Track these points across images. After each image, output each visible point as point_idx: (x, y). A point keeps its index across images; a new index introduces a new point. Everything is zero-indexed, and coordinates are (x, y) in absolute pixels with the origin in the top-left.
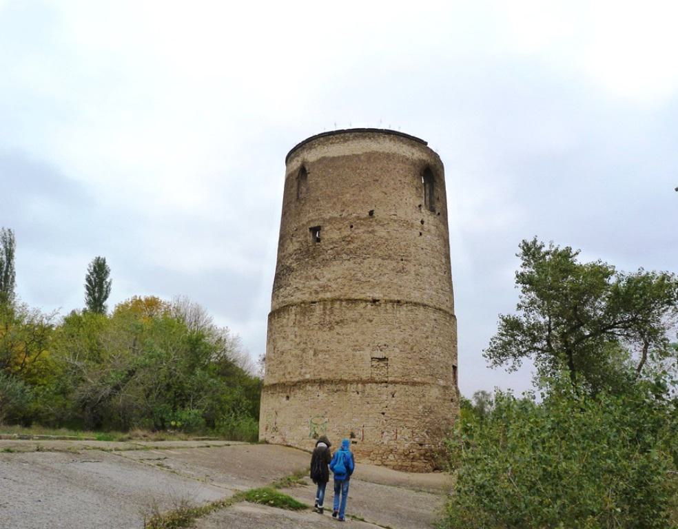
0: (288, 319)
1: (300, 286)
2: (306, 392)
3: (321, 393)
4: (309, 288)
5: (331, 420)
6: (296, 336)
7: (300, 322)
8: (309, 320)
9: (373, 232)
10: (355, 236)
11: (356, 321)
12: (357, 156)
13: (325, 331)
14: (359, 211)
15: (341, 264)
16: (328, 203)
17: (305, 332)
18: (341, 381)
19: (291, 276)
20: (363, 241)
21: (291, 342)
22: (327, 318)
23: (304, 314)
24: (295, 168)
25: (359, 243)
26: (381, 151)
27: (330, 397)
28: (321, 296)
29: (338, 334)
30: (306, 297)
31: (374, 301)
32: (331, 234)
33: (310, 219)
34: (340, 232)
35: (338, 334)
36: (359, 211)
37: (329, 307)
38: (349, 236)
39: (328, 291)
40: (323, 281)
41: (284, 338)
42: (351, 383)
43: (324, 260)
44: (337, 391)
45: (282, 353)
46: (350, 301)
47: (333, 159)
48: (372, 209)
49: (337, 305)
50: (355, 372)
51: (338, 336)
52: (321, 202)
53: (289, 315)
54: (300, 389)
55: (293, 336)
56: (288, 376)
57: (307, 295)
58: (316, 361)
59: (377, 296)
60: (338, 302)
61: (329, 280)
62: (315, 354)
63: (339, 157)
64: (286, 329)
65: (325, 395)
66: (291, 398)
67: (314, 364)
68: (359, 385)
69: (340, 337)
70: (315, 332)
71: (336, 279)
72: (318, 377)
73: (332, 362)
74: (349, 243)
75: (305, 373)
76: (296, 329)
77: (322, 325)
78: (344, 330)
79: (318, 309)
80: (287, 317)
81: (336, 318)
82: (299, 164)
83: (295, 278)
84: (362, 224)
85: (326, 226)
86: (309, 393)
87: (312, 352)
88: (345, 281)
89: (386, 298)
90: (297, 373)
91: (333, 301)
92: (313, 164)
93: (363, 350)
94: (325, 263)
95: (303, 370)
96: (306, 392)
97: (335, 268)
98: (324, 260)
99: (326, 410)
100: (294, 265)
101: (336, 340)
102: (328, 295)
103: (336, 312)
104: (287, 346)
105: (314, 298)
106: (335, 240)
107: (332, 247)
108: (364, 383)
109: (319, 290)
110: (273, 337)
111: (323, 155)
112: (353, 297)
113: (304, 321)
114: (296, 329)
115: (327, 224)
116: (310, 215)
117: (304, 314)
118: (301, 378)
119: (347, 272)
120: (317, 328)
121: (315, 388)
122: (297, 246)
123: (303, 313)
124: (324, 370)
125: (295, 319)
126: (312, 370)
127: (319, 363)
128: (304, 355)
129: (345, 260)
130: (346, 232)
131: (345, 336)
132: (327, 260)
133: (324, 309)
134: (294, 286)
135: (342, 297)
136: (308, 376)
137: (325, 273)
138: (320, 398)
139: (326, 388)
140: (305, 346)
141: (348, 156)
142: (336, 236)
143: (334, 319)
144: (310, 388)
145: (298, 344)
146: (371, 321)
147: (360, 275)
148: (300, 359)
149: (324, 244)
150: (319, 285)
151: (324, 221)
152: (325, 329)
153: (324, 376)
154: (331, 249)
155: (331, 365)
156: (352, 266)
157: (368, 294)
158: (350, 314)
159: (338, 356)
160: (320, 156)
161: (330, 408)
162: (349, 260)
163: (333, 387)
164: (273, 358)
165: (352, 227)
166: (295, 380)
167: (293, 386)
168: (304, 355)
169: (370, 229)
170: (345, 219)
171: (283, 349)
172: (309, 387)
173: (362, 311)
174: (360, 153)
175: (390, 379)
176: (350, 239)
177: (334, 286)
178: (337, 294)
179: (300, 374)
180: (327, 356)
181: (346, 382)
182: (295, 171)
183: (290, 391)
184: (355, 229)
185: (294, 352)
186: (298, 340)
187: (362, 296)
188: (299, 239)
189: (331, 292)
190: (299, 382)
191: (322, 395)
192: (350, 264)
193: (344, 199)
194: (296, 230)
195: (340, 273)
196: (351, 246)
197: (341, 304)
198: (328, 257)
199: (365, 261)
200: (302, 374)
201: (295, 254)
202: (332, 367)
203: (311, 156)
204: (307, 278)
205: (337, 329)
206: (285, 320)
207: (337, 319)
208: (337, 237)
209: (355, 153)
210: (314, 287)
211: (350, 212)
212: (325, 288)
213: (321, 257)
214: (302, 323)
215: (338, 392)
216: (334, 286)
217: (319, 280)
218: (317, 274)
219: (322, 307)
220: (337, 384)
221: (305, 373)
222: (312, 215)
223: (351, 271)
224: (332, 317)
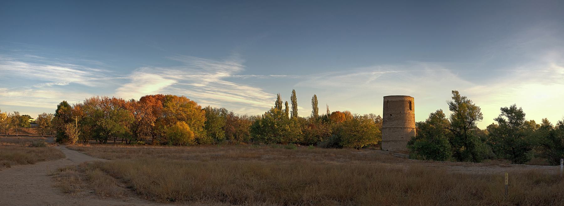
18: (396, 141)
31: (401, 128)
32: (393, 116)
45: (386, 136)
46: (397, 128)
49: (395, 128)
74: (397, 118)
82: (387, 100)
91: (394, 128)
102: (394, 127)
108: (400, 141)
112: (398, 127)
122: (388, 117)
139: (394, 142)
177: (394, 125)
178: (395, 127)
181: (397, 141)
191: (393, 143)
196: (397, 118)
203: (390, 100)
205: (395, 132)
212: (393, 125)
220: (396, 141)
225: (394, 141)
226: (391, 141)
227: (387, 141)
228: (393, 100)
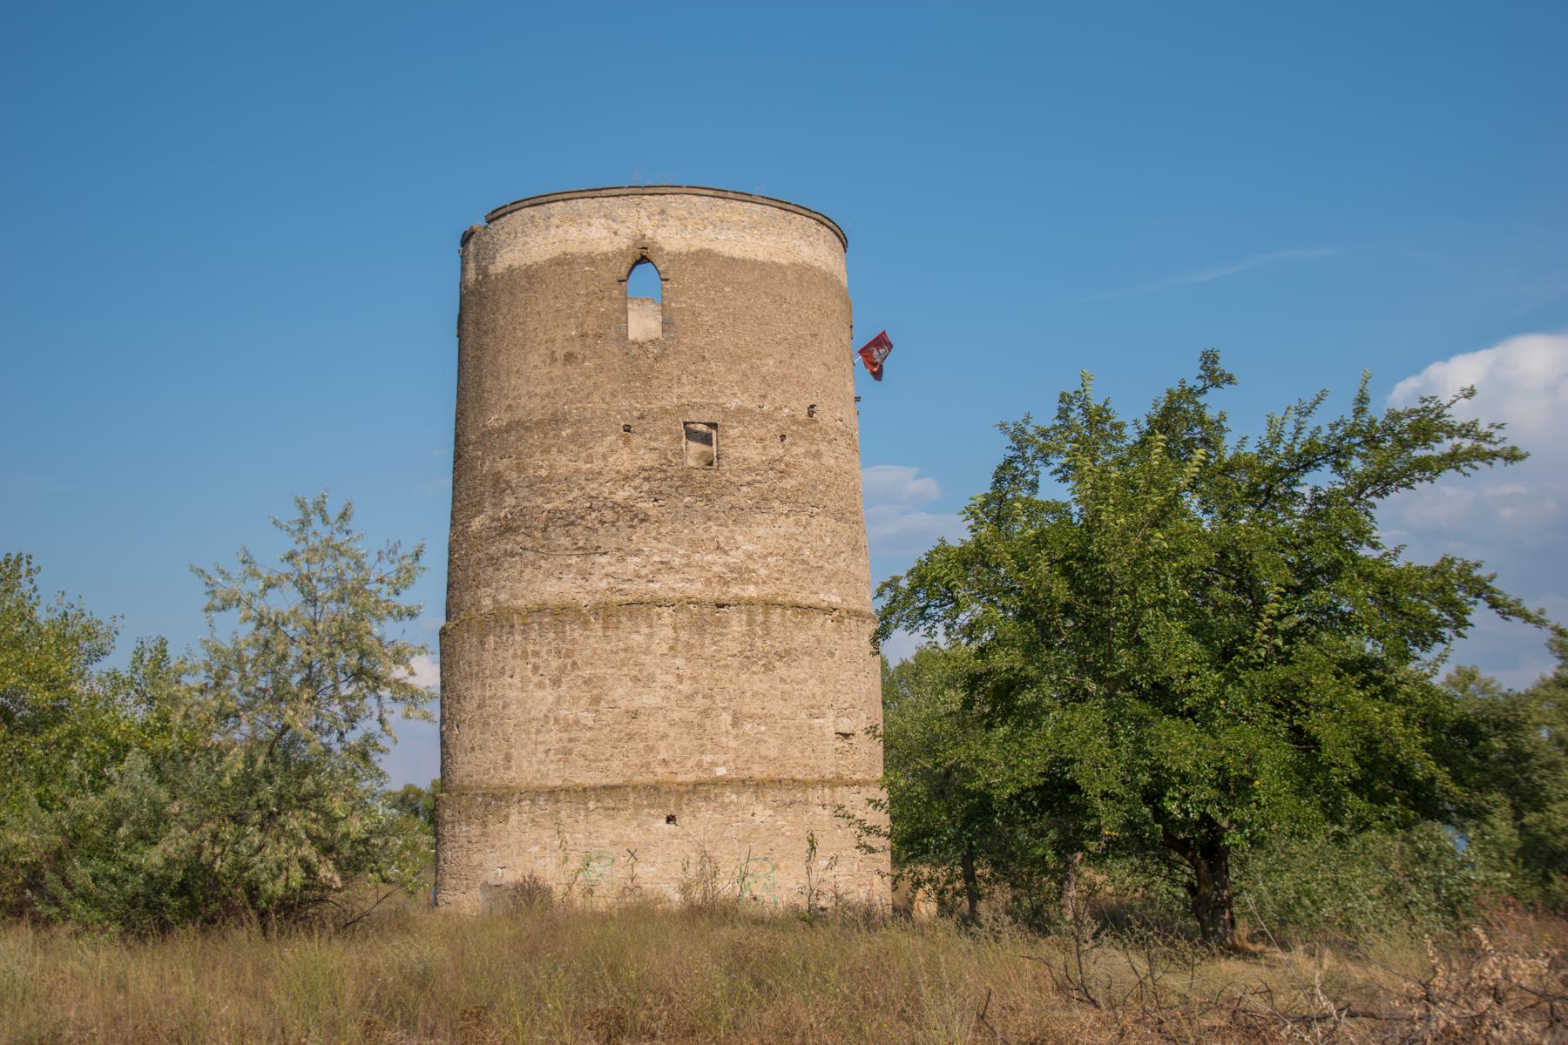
0: (651, 636)
1: (677, 562)
2: (724, 806)
3: (759, 809)
4: (702, 568)
5: (782, 865)
6: (680, 678)
7: (689, 646)
8: (715, 643)
9: (817, 455)
10: (791, 460)
11: (810, 655)
12: (780, 267)
13: (754, 673)
14: (794, 404)
15: (773, 521)
16: (729, 370)
17: (706, 672)
19: (640, 532)
20: (805, 474)
21: (663, 692)
22: (759, 643)
23: (702, 630)
24: (606, 247)
25: (801, 480)
26: (816, 264)
27: (779, 817)
28: (735, 590)
29: (782, 680)
30: (696, 589)
33: (684, 401)
34: (764, 448)
35: (782, 680)
36: (794, 404)
37: (760, 618)
38: (781, 460)
39: (749, 581)
40: (735, 557)
41: (636, 679)
42: (813, 784)
43: (732, 507)
44: (791, 803)
45: (635, 715)
47: (731, 262)
48: (812, 403)
49: (776, 616)
50: (812, 762)
51: (780, 686)
52: (713, 364)
53: (651, 626)
54: (706, 799)
55: (671, 679)
56: (659, 770)
57: (699, 585)
58: (736, 737)
59: (835, 599)
60: (779, 610)
61: (750, 556)
62: (736, 723)
63: (744, 261)
64: (647, 659)
65: (769, 812)
66: (684, 819)
67: (733, 744)
68: (826, 790)
69: (787, 687)
70: (731, 673)
71: (765, 557)
72: (745, 774)
73: (772, 741)
75: (714, 764)
76: (679, 662)
77: (747, 659)
78: (793, 672)
79: (737, 623)
80: (645, 630)
81: (777, 645)
83: (659, 541)
84: (802, 437)
85: (732, 427)
86: (732, 807)
87: (726, 718)
88: (783, 563)
89: (845, 605)
90: (690, 763)
91: (769, 605)
92: (676, 258)
93: (823, 715)
94: (739, 514)
95: (708, 758)
96: (724, 806)
97: (761, 531)
98: (732, 507)
99: (773, 846)
100: (647, 506)
101: (779, 693)
102: (751, 591)
103: (776, 630)
104: (650, 699)
105: (716, 593)
106: (753, 464)
107: (749, 479)
109: (729, 576)
110: (587, 673)
111: (706, 245)
112: (802, 598)
113: (702, 646)
114: (679, 662)
115: (735, 424)
116: (687, 389)
117: (702, 630)
118: (704, 776)
119: (785, 543)
120: (736, 664)
121: (744, 799)
122: (650, 459)
123: (700, 627)
124: (757, 757)
125: (676, 639)
126: (730, 756)
127: (746, 744)
128: (708, 722)
129: (781, 514)
130: (777, 451)
131: (794, 685)
132: (742, 509)
133: (750, 623)
134: (657, 558)
135: (780, 599)
136: (721, 771)
137: (739, 538)
138: (757, 819)
139: (770, 795)
140: (708, 702)
141: (763, 264)
142: (754, 454)
143: (771, 646)
144: (734, 797)
145: (691, 697)
146: (832, 654)
147: (807, 552)
148: (696, 731)
149: (731, 471)
150: (726, 565)
151: (725, 411)
152: (754, 669)
153: (758, 771)
154: (748, 484)
155: (771, 748)
156: (793, 530)
157: (822, 596)
158: (800, 638)
159: (785, 727)
160: (697, 244)
161: (780, 840)
162: (787, 515)
163: (786, 797)
164: (591, 723)
165: (783, 437)
166: (691, 778)
167: (688, 792)
168: (708, 722)
169: (814, 449)
170: (767, 417)
171: (636, 704)
172: (730, 796)
173: (819, 632)
174: (784, 262)
175: (858, 776)
176: (783, 466)
178: (768, 590)
179: (699, 765)
180: (763, 728)
182: (606, 258)
183: (678, 806)
184: (791, 444)
185: (676, 716)
186: (686, 687)
187: (813, 600)
188: (653, 444)
189: (756, 583)
190: (697, 784)
192: (786, 525)
193: (764, 370)
194: (642, 417)
195: (771, 542)
196: (789, 483)
197: (783, 615)
198: (743, 505)
199: (814, 521)
200: (705, 765)
201: (646, 479)
202: (773, 753)
204: (695, 545)
205: (781, 668)
206: (636, 637)
207: (779, 647)
208: (758, 459)
209: (776, 260)
210: (715, 569)
211: (778, 403)
212: (742, 574)
213: (726, 498)
214: (697, 651)
215: (795, 807)
216: (763, 572)
217: (726, 553)
218: (721, 539)
219: (744, 617)
221: (714, 764)
222: (687, 391)
223: (792, 542)
224: (768, 642)
225: (777, 783)
226: (727, 783)
227: (655, 788)
228: (717, 247)
